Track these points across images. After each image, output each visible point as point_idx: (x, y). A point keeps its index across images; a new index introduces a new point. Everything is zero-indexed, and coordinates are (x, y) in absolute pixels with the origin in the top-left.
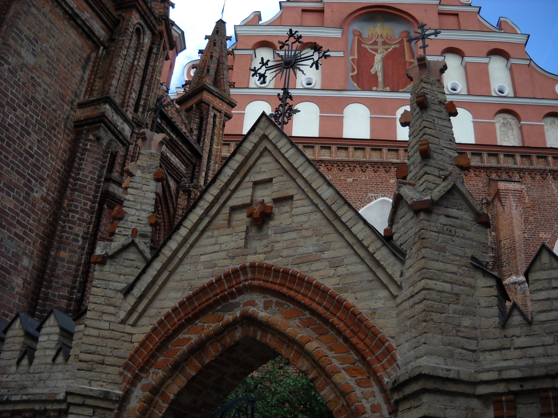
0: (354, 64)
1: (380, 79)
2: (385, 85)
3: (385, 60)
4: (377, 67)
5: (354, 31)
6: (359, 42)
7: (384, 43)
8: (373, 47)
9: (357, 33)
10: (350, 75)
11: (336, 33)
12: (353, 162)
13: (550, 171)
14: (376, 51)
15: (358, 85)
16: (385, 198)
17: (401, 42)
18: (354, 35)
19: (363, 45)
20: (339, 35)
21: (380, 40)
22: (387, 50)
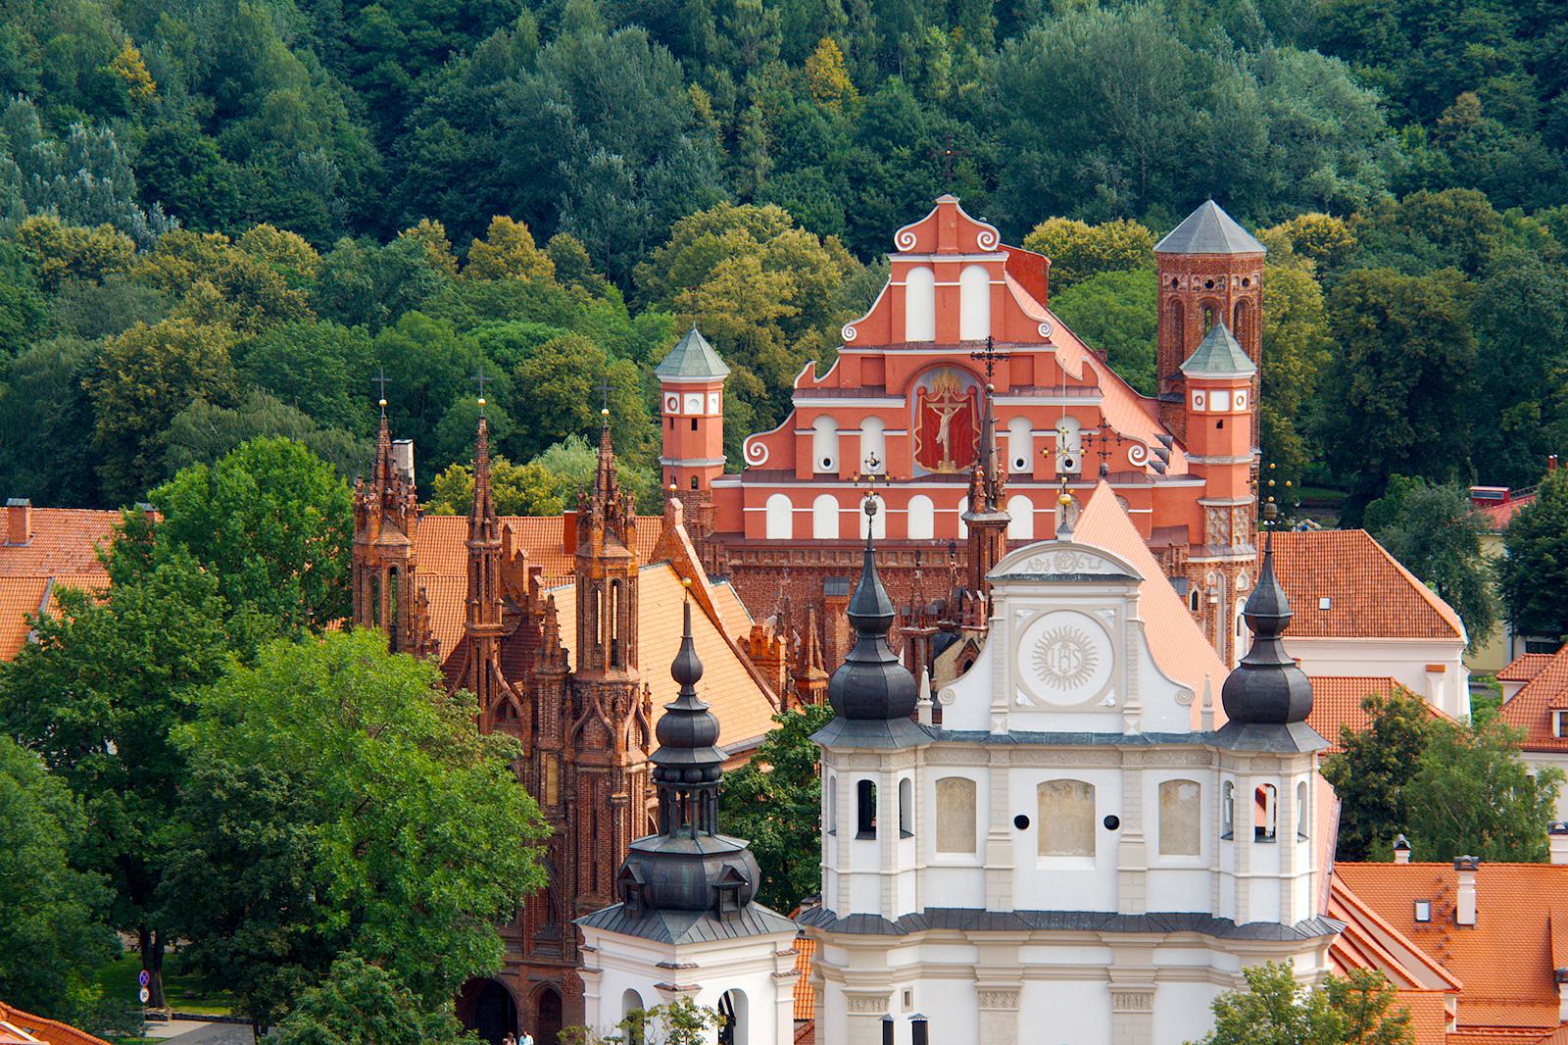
1: (946, 450)
2: (951, 458)
3: (952, 422)
4: (943, 434)
6: (925, 402)
7: (951, 400)
8: (939, 405)
11: (899, 403)
14: (942, 410)
17: (968, 401)
21: (947, 395)
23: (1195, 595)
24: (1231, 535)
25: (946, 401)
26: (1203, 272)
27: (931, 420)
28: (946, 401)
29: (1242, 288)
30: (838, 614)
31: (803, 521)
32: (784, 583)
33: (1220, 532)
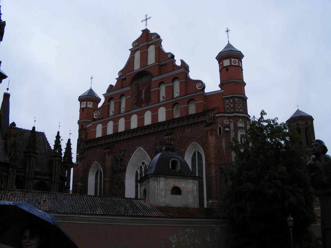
1: (144, 101)
2: (145, 103)
4: (143, 95)
8: (142, 88)
10: (134, 103)
11: (129, 88)
13: (186, 125)
14: (143, 89)
15: (137, 106)
16: (140, 148)
17: (149, 84)
18: (136, 85)
21: (144, 84)
22: (146, 87)
23: (220, 129)
24: (234, 106)
27: (139, 92)
29: (306, 124)
30: (107, 156)
31: (104, 130)
32: (98, 150)
33: (230, 107)
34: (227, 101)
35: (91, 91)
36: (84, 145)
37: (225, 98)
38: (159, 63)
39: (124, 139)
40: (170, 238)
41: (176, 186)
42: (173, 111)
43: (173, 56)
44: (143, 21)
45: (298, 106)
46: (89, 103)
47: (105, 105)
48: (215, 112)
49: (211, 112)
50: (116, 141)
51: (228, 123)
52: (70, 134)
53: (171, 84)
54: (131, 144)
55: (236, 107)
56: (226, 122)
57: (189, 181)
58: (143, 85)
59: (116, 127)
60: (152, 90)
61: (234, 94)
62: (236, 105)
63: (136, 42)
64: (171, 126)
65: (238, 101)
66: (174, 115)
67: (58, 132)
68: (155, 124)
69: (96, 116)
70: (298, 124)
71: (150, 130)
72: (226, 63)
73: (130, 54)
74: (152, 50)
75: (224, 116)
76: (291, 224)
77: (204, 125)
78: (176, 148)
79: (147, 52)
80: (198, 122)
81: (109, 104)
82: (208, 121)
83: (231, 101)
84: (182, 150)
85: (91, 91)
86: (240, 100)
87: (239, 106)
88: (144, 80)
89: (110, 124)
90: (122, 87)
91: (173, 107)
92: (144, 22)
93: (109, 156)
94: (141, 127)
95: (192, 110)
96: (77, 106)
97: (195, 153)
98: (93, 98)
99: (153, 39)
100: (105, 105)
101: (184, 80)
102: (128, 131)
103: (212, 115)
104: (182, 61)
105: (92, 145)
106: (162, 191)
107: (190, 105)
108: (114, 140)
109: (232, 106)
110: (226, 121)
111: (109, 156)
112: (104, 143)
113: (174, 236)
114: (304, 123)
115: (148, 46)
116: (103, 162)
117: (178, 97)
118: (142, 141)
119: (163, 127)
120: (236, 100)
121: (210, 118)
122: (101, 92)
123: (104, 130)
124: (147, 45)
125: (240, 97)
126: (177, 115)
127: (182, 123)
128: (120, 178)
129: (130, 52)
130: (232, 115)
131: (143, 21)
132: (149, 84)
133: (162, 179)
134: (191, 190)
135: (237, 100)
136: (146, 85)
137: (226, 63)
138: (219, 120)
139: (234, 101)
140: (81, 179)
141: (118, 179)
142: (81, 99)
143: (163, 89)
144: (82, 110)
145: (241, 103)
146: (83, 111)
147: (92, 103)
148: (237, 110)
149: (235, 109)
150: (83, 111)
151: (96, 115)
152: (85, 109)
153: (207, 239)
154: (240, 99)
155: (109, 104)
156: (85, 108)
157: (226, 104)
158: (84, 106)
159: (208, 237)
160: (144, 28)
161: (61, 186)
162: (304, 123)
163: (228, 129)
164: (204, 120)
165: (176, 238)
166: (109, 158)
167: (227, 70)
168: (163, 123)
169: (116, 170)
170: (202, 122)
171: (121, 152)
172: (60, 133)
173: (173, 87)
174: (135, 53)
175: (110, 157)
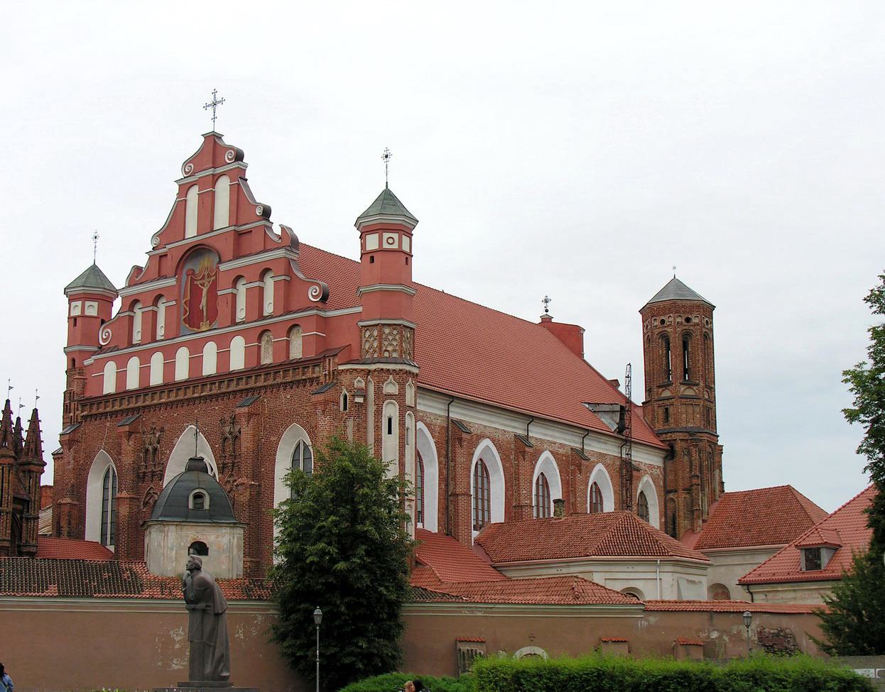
0: (187, 305)
1: (205, 314)
3: (208, 292)
5: (189, 270)
6: (192, 280)
8: (201, 282)
9: (192, 271)
11: (171, 282)
12: (176, 401)
13: (281, 383)
14: (203, 285)
17: (216, 275)
18: (188, 275)
19: (195, 282)
20: (175, 283)
21: (206, 273)
22: (209, 282)
23: (345, 397)
24: (380, 348)
25: (206, 277)
26: (658, 315)
27: (195, 292)
28: (206, 277)
29: (685, 323)
31: (121, 377)
32: (108, 424)
34: (368, 334)
35: (94, 271)
36: (78, 410)
37: (362, 326)
38: (237, 228)
39: (160, 404)
40: (171, 633)
41: (198, 540)
42: (259, 348)
43: (267, 213)
44: (206, 107)
45: (674, 268)
46: (88, 303)
47: (121, 315)
48: (336, 360)
49: (330, 359)
50: (144, 407)
51: (363, 385)
52: (38, 397)
53: (257, 284)
54: (176, 415)
55: (384, 348)
56: (359, 383)
57: (224, 531)
58: (204, 275)
59: (145, 372)
60: (219, 293)
61: (380, 319)
62: (386, 343)
63: (190, 162)
64: (252, 384)
65: (390, 334)
66: (262, 357)
67: (8, 401)
68: (225, 376)
69: (104, 340)
70: (663, 322)
71: (214, 386)
72: (373, 242)
73: (178, 192)
74: (223, 186)
75: (354, 370)
76: (318, 620)
77: (315, 387)
78: (262, 433)
79: (214, 193)
80: (304, 380)
81: (132, 314)
82: (322, 379)
83: (375, 333)
84: (273, 439)
85: (94, 271)
86: (395, 332)
87: (391, 345)
88: (202, 265)
89: (134, 365)
90: (161, 277)
91: (259, 339)
92: (210, 109)
93: (128, 440)
94: (197, 381)
95: (296, 352)
96: (60, 309)
97: (298, 446)
98: (100, 293)
99: (229, 162)
100: (121, 315)
101: (283, 278)
102: (170, 386)
103: (331, 365)
104: (283, 228)
105: (94, 412)
106: (172, 549)
107: (293, 337)
108: (139, 404)
109: (375, 344)
110: (359, 381)
111: (128, 440)
112: (120, 408)
113: (179, 629)
114: (679, 320)
115: (215, 179)
116: (116, 452)
117: (271, 317)
118: (196, 411)
119: (238, 384)
120: (384, 333)
121: (327, 372)
122: (118, 278)
123: (121, 377)
124: (214, 175)
125: (395, 324)
126: (267, 359)
127: (274, 380)
128: (152, 492)
129: (175, 189)
130: (373, 367)
131: (206, 107)
132: (216, 275)
133: (173, 528)
134: (225, 547)
135: (387, 331)
136: (209, 276)
137: (373, 242)
138: (345, 379)
139: (380, 335)
140: (73, 485)
141: (148, 493)
142: (75, 294)
143: (242, 289)
144: (73, 321)
145: (397, 338)
146: (75, 325)
147: (95, 304)
148: (386, 354)
149: (380, 354)
150: (75, 325)
151: (104, 337)
152: (79, 321)
153: (237, 635)
154: (394, 329)
155: (132, 314)
156: (79, 316)
157: (364, 340)
158: (77, 312)
159: (240, 632)
160: (209, 130)
161: (18, 516)
162: (679, 320)
163: (360, 400)
164: (315, 376)
165: (182, 633)
166: (128, 446)
167: (372, 259)
168: (238, 376)
169: (144, 473)
170: (311, 380)
171: (154, 433)
172: (11, 403)
173: (261, 289)
174: (188, 189)
175: (131, 443)
